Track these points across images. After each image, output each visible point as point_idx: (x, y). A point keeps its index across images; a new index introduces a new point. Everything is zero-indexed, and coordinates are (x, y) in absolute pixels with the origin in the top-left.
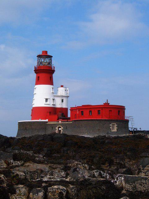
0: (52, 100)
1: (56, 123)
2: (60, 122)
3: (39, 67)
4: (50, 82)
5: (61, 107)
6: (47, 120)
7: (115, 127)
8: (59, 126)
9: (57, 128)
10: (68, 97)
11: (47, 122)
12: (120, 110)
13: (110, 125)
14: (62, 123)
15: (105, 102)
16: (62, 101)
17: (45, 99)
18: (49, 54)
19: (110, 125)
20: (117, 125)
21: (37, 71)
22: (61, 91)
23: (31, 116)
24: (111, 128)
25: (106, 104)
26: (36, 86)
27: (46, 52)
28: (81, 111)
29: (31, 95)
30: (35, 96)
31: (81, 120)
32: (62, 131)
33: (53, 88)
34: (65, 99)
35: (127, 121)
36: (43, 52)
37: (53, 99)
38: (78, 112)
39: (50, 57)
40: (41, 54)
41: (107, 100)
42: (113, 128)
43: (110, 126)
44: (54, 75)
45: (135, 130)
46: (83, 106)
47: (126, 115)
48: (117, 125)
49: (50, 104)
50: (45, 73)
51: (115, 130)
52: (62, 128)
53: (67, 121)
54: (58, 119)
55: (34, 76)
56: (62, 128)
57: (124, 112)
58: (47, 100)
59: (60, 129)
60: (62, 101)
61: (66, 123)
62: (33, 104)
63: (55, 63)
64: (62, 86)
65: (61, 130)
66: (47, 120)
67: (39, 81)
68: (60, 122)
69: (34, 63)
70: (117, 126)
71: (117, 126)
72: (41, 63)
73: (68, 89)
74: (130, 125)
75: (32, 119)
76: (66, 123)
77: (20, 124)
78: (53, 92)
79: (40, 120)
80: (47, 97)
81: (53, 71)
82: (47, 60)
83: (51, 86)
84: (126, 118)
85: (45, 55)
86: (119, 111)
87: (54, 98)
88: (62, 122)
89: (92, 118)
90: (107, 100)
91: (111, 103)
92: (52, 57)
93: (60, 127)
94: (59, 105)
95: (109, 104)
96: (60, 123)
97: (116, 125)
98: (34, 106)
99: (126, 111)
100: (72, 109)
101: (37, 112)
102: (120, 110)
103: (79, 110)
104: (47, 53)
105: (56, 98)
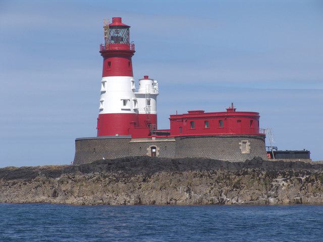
0: (133, 102)
1: (147, 141)
2: (154, 139)
4: (127, 71)
5: (148, 113)
8: (152, 146)
9: (149, 149)
12: (253, 118)
13: (240, 143)
14: (157, 141)
15: (229, 106)
16: (149, 103)
18: (124, 22)
19: (240, 143)
20: (249, 144)
21: (106, 53)
22: (146, 87)
24: (241, 148)
25: (232, 109)
26: (105, 79)
27: (120, 19)
32: (158, 154)
33: (133, 82)
34: (152, 101)
35: (262, 137)
36: (114, 19)
37: (135, 101)
39: (127, 27)
41: (232, 104)
44: (133, 58)
45: (274, 150)
46: (189, 112)
47: (261, 127)
48: (249, 144)
49: (130, 108)
50: (118, 57)
52: (158, 149)
55: (102, 58)
56: (158, 149)
58: (125, 102)
59: (154, 150)
60: (149, 103)
63: (135, 38)
64: (146, 78)
65: (155, 153)
73: (155, 82)
74: (268, 142)
81: (132, 53)
82: (121, 33)
83: (131, 79)
84: (261, 132)
85: (117, 25)
90: (232, 104)
91: (239, 109)
94: (142, 108)
95: (235, 109)
96: (153, 141)
97: (248, 143)
99: (260, 120)
100: (173, 119)
101: (106, 122)
102: (253, 118)
105: (139, 99)
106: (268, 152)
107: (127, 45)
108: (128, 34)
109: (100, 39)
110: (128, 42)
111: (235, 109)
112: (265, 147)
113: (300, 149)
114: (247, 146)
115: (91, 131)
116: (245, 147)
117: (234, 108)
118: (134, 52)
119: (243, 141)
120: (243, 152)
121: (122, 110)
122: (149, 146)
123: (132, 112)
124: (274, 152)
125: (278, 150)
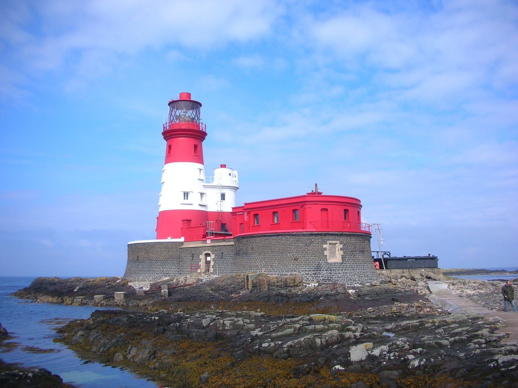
2: (209, 241)
6: (182, 239)
7: (337, 252)
9: (202, 257)
10: (236, 189)
11: (182, 243)
12: (350, 207)
13: (325, 246)
16: (223, 197)
19: (325, 246)
20: (341, 246)
21: (169, 134)
22: (223, 177)
23: (156, 230)
24: (326, 253)
25: (315, 193)
28: (252, 213)
29: (156, 185)
30: (164, 187)
31: (252, 236)
32: (212, 263)
35: (367, 236)
37: (202, 194)
38: (246, 218)
39: (196, 105)
41: (316, 185)
42: (333, 254)
43: (325, 249)
44: (204, 143)
45: (386, 256)
48: (341, 246)
49: (194, 204)
51: (337, 258)
53: (224, 240)
54: (205, 236)
55: (164, 144)
56: (213, 256)
57: (359, 212)
58: (186, 195)
59: (209, 259)
60: (223, 197)
61: (221, 244)
62: (159, 204)
63: (207, 119)
64: (223, 166)
66: (182, 239)
67: (171, 156)
68: (209, 241)
69: (163, 117)
70: (341, 249)
71: (341, 249)
72: (178, 117)
75: (157, 239)
76: (221, 244)
77: (133, 249)
78: (202, 177)
79: (169, 240)
86: (346, 211)
90: (316, 185)
92: (200, 105)
93: (207, 255)
95: (320, 193)
97: (339, 246)
98: (161, 209)
99: (363, 211)
103: (249, 213)
104: (190, 98)
106: (376, 260)
112: (370, 252)
113: (424, 254)
114: (337, 250)
116: (335, 251)
117: (319, 191)
119: (331, 242)
120: (331, 261)
122: (202, 252)
123: (196, 207)
124: (384, 259)
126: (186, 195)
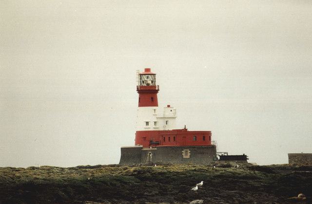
2: (151, 148)
3: (141, 87)
6: (141, 146)
11: (142, 148)
17: (145, 123)
18: (152, 72)
39: (154, 75)
40: (142, 71)
42: (186, 154)
44: (159, 95)
45: (226, 155)
49: (151, 127)
54: (150, 145)
55: (137, 95)
58: (147, 123)
67: (142, 103)
68: (151, 148)
80: (147, 121)
81: (157, 91)
84: (212, 143)
87: (156, 121)
88: (152, 148)
89: (169, 144)
93: (150, 153)
95: (187, 129)
107: (155, 87)
108: (155, 79)
109: (135, 83)
110: (155, 84)
111: (187, 129)
115: (131, 143)
118: (158, 90)
120: (184, 157)
121: (146, 128)
123: (152, 129)
125: (228, 155)
126: (147, 123)
